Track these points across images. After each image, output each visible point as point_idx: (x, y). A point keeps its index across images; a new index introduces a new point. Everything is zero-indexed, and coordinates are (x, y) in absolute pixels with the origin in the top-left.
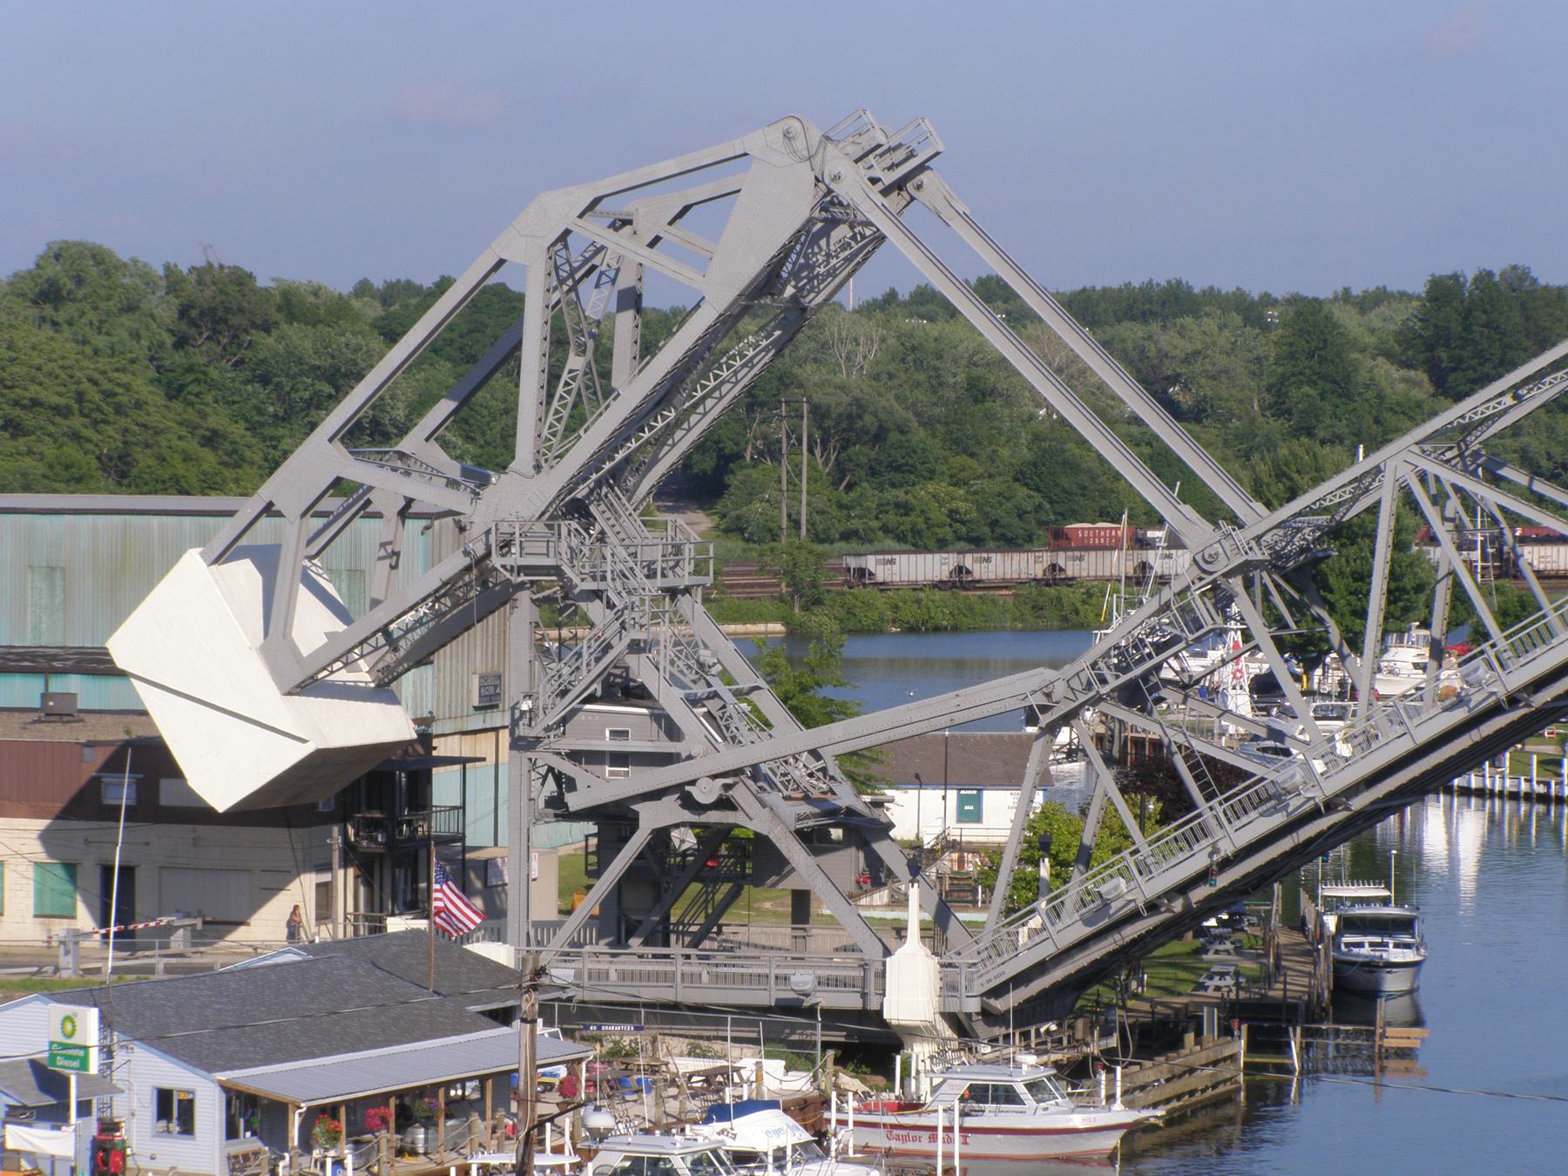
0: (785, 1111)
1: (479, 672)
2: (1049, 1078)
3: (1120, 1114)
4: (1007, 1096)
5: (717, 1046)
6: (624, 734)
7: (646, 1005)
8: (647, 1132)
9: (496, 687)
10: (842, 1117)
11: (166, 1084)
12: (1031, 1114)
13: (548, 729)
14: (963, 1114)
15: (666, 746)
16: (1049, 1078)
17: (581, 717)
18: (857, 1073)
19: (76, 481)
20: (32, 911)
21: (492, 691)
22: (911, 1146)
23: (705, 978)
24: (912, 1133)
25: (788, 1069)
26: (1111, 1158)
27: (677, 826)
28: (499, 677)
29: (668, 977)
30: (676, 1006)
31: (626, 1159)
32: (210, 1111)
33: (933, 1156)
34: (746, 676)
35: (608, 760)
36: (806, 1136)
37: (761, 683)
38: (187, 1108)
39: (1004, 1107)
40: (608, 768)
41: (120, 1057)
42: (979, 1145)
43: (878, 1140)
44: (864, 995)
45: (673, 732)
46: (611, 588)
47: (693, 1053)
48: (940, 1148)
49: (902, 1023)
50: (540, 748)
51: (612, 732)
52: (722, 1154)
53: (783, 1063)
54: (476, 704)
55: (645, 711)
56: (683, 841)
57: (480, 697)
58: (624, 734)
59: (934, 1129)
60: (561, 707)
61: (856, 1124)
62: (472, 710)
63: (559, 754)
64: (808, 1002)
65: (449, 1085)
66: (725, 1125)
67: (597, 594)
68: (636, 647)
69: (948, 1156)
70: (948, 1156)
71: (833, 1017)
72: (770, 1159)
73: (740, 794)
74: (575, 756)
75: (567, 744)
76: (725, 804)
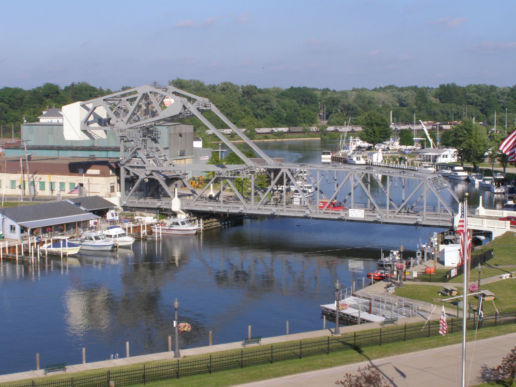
1: (180, 149)
2: (186, 221)
6: (137, 163)
11: (12, 224)
12: (181, 227)
16: (186, 221)
19: (205, 117)
23: (150, 203)
26: (197, 234)
32: (18, 229)
38: (14, 228)
41: (5, 220)
45: (145, 163)
67: (132, 141)
73: (154, 173)
74: (131, 167)
75: (129, 165)
76: (151, 174)
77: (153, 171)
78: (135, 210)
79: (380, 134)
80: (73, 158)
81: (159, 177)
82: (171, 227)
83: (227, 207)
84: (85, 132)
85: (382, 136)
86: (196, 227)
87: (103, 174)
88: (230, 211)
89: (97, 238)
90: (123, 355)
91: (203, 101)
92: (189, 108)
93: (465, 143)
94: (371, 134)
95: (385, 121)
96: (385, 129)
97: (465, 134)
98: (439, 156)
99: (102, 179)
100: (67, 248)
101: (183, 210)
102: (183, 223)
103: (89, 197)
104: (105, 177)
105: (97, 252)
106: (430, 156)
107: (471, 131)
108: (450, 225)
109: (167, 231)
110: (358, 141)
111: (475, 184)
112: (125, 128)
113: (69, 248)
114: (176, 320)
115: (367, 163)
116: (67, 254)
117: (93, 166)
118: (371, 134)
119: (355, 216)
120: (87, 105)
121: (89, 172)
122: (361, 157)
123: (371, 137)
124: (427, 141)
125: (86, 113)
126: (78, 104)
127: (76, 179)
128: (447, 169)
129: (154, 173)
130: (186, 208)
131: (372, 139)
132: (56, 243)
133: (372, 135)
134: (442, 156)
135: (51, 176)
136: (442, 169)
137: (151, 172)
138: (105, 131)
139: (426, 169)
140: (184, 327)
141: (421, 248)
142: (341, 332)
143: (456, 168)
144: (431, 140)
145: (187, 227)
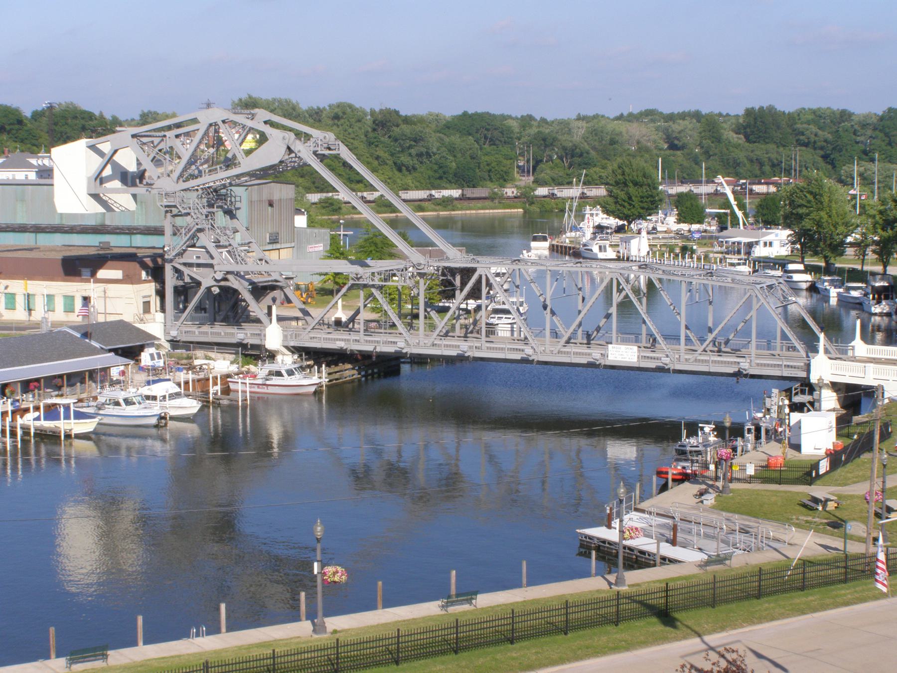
1: (270, 231)
2: (295, 369)
6: (198, 257)
12: (287, 380)
15: (210, 261)
16: (295, 369)
20: (63, 310)
26: (317, 393)
27: (213, 286)
45: (212, 258)
67: (188, 214)
73: (230, 277)
74: (185, 264)
76: (225, 279)
77: (228, 273)
78: (194, 347)
79: (641, 202)
80: (66, 248)
81: (241, 284)
82: (267, 380)
83: (372, 342)
84: (96, 197)
85: (645, 205)
86: (315, 380)
87: (129, 279)
88: (378, 349)
89: (128, 402)
90: (214, 630)
91: (325, 138)
92: (299, 151)
93: (810, 219)
94: (624, 201)
95: (651, 178)
96: (650, 193)
97: (809, 202)
98: (757, 243)
99: (127, 289)
100: (72, 421)
101: (287, 347)
102: (290, 373)
103: (106, 323)
104: (132, 283)
105: (127, 429)
106: (739, 243)
107: (821, 195)
108: (803, 374)
109: (258, 388)
110: (597, 215)
111: (829, 297)
112: (173, 190)
113: (77, 421)
114: (318, 561)
115: (619, 257)
116: (73, 433)
117: (110, 263)
118: (624, 201)
119: (619, 358)
120: (100, 146)
121: (102, 274)
122: (607, 246)
123: (624, 207)
124: (733, 214)
125: (98, 161)
126: (81, 144)
127: (76, 288)
128: (773, 268)
129: (230, 277)
130: (292, 344)
131: (626, 211)
132: (51, 412)
133: (626, 204)
134: (762, 243)
135: (29, 282)
136: (765, 267)
137: (225, 274)
138: (134, 196)
139: (732, 268)
140: (335, 573)
141: (754, 418)
142: (627, 582)
143: (791, 267)
144: (739, 214)
145: (298, 379)
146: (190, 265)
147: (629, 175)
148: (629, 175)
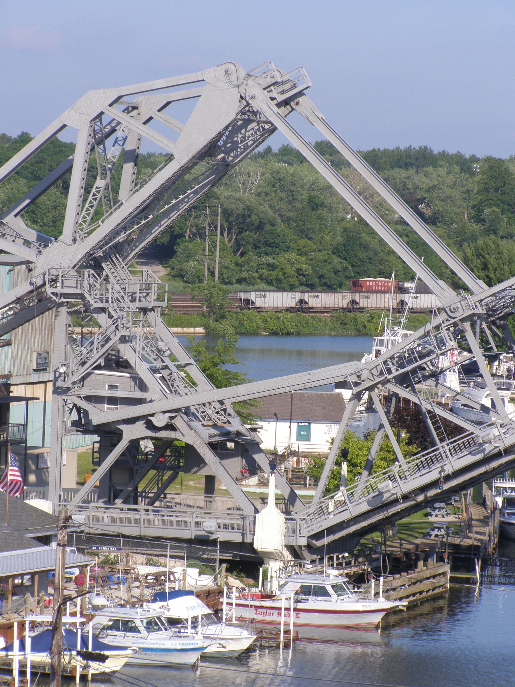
0: (198, 596)
1: (37, 350)
2: (344, 583)
3: (383, 603)
4: (321, 592)
5: (162, 560)
6: (115, 387)
7: (124, 536)
8: (122, 606)
9: (46, 359)
10: (229, 601)
13: (74, 383)
14: (297, 601)
15: (138, 394)
16: (344, 583)
17: (92, 377)
18: (238, 577)
21: (43, 361)
22: (268, 618)
23: (156, 522)
24: (269, 611)
25: (200, 573)
26: (377, 627)
27: (143, 438)
28: (48, 353)
29: (136, 521)
30: (140, 538)
31: (110, 620)
33: (279, 623)
34: (183, 358)
35: (106, 402)
36: (208, 611)
37: (192, 361)
39: (320, 598)
40: (106, 406)
42: (305, 618)
43: (249, 614)
44: (243, 534)
45: (142, 386)
46: (111, 307)
47: (149, 563)
48: (283, 619)
49: (263, 550)
50: (69, 393)
51: (109, 386)
52: (163, 619)
53: (197, 570)
54: (35, 368)
55: (127, 375)
56: (146, 447)
57: (37, 364)
58: (115, 387)
59: (280, 609)
60: (82, 371)
61: (237, 605)
62: (32, 371)
63: (80, 397)
64: (212, 537)
65: (14, 577)
66: (164, 603)
67: (103, 310)
68: (123, 340)
69: (287, 624)
70: (287, 624)
71: (226, 546)
72: (190, 623)
73: (178, 422)
74: (88, 398)
75: (85, 392)
76: (169, 427)
122: (506, 401)
146: (98, 400)
147: (495, 270)
148: (495, 270)
